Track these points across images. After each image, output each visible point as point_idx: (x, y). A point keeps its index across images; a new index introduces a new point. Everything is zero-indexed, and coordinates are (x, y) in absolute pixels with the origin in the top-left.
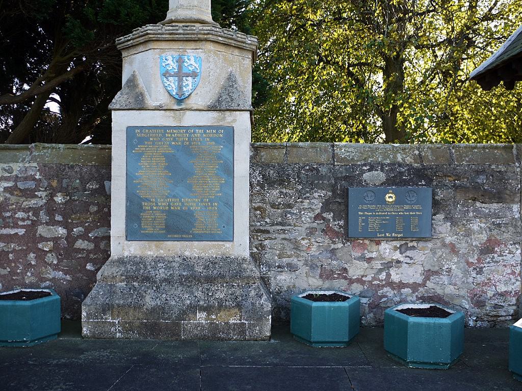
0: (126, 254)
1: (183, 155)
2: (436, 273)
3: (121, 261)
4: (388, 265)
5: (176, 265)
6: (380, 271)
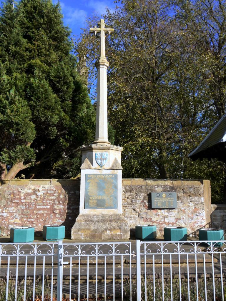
0: (84, 213)
1: (103, 183)
2: (179, 219)
3: (83, 216)
4: (164, 217)
5: (100, 216)
6: (162, 219)
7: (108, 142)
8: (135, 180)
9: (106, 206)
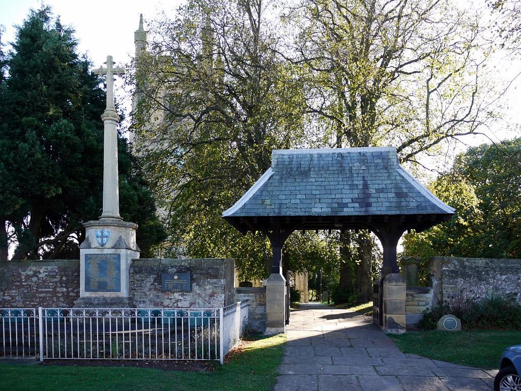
0: (85, 296)
2: (194, 303)
3: (83, 298)
4: (177, 301)
5: (101, 299)
6: (175, 303)
7: (120, 217)
8: (147, 260)
9: (108, 288)
